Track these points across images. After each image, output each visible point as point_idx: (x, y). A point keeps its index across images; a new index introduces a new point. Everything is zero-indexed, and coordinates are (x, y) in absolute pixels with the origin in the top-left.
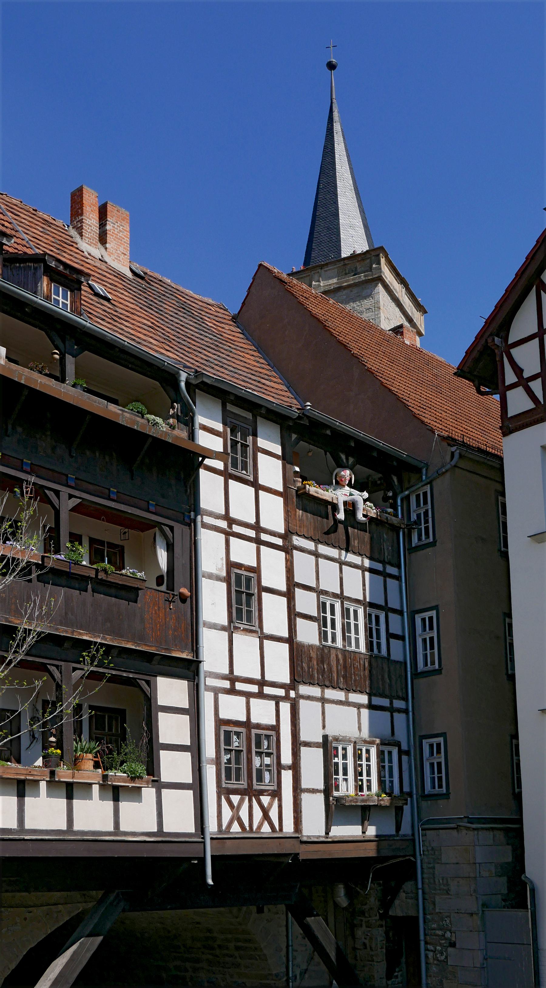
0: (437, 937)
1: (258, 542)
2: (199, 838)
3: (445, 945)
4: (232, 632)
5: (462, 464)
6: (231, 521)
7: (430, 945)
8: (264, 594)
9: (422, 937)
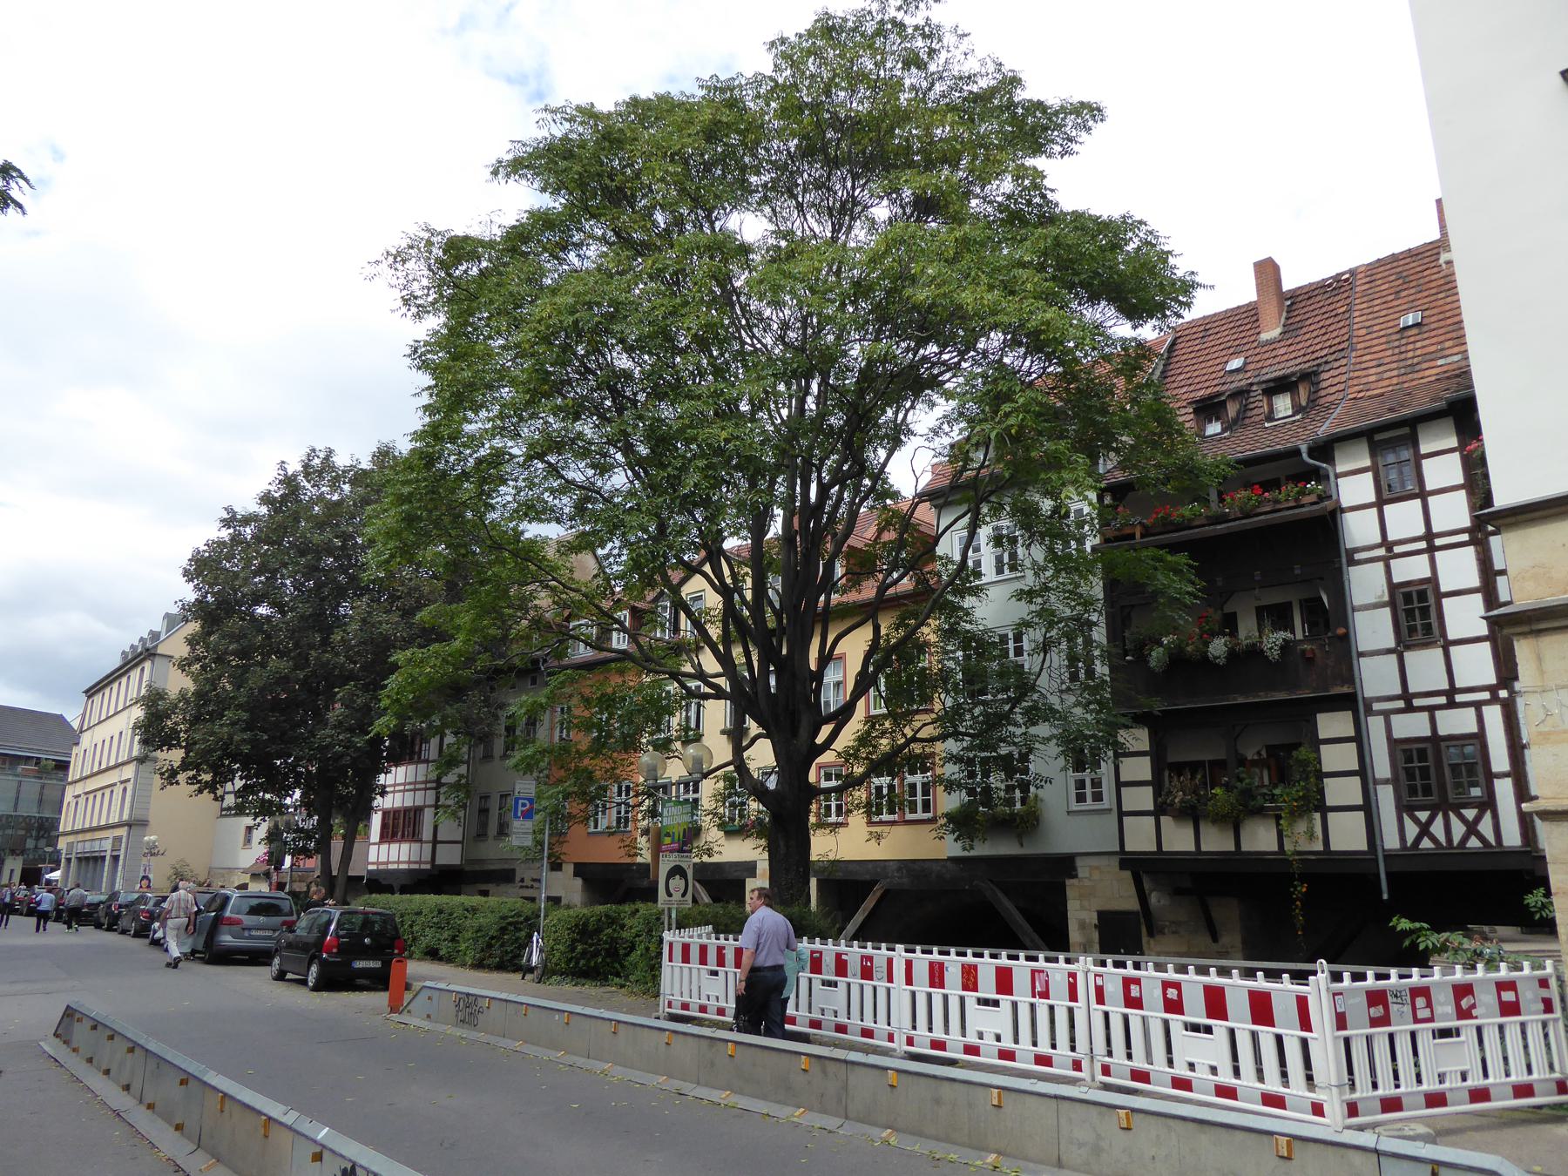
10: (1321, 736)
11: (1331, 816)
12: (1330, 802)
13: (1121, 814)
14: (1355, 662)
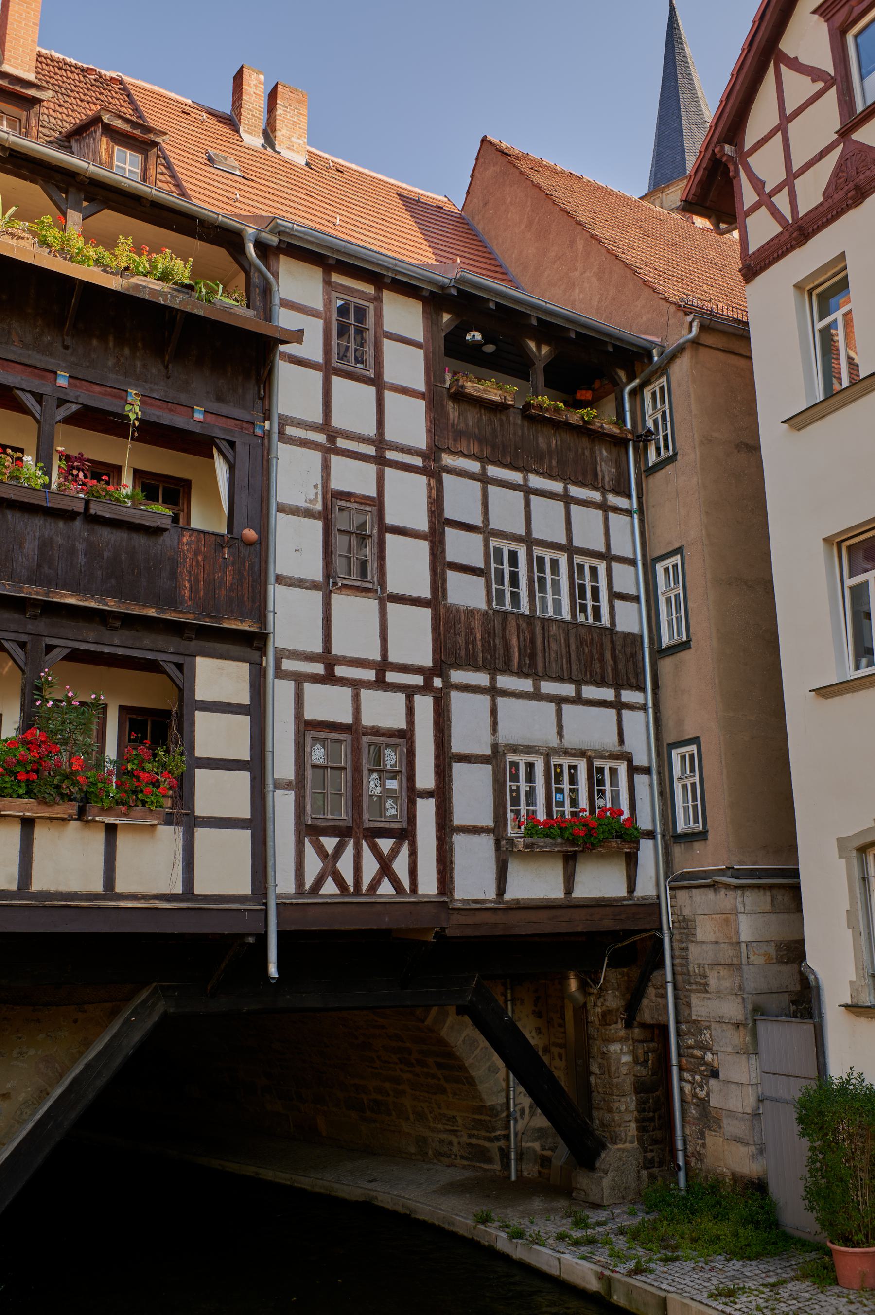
0: (695, 1060)
1: (381, 461)
2: (259, 904)
3: (705, 1073)
4: (331, 592)
5: (708, 339)
6: (333, 434)
7: (687, 1073)
8: (388, 536)
9: (674, 1059)
10: (201, 694)
11: (200, 833)
12: (201, 809)
14: (271, 588)
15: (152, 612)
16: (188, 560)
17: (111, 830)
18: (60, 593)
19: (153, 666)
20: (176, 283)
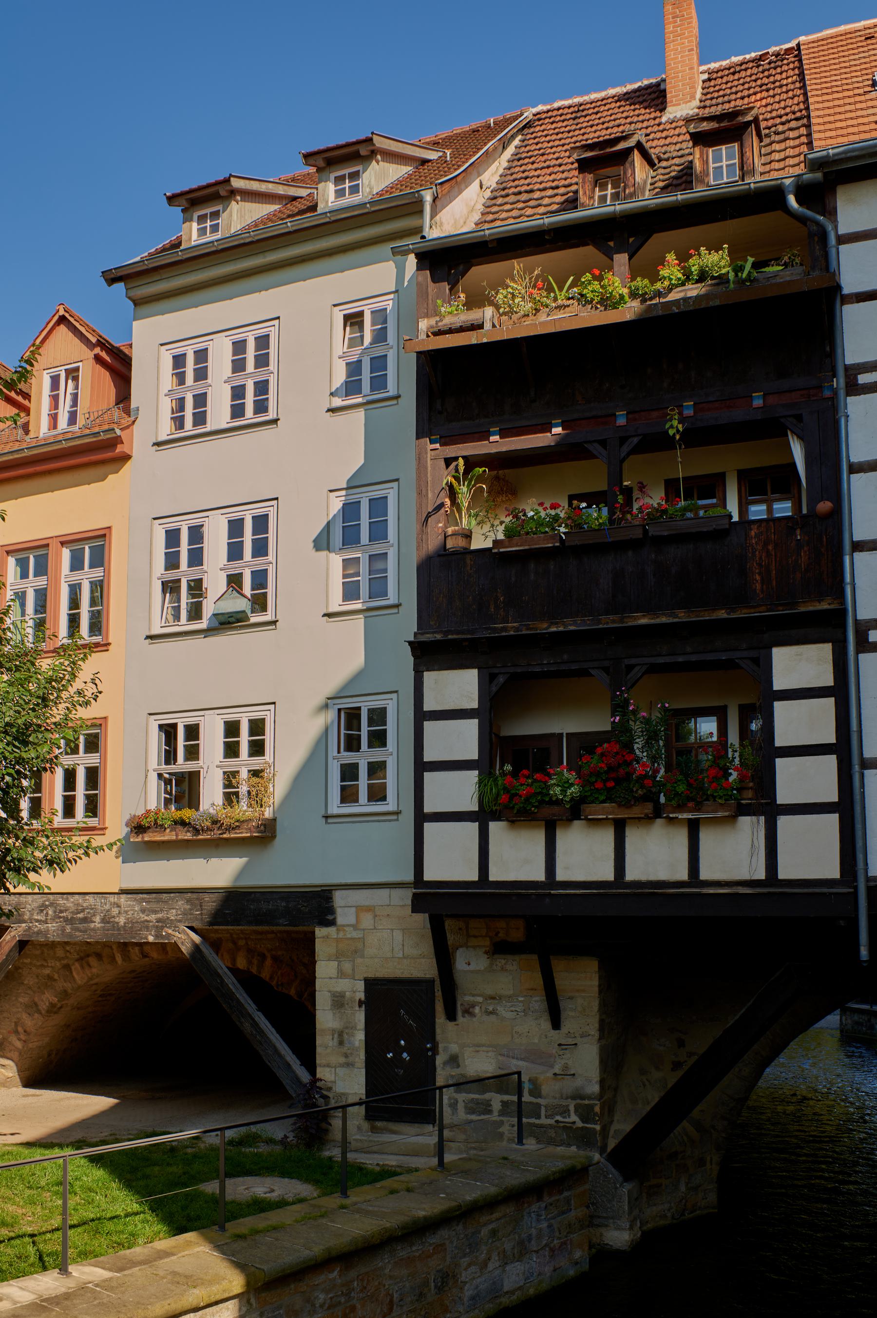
13: (421, 818)
15: (722, 614)
16: (757, 552)
17: (694, 828)
18: (634, 616)
19: (730, 665)
20: (713, 278)
